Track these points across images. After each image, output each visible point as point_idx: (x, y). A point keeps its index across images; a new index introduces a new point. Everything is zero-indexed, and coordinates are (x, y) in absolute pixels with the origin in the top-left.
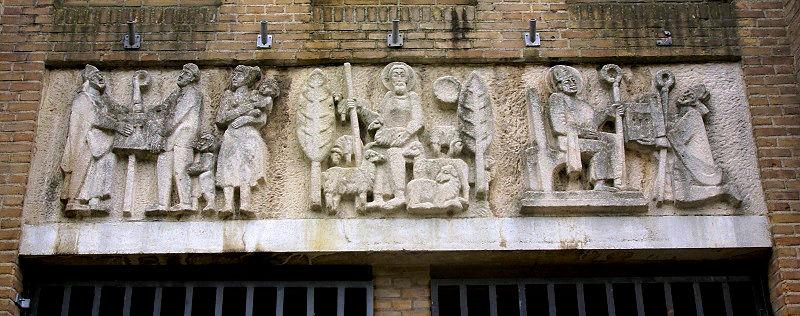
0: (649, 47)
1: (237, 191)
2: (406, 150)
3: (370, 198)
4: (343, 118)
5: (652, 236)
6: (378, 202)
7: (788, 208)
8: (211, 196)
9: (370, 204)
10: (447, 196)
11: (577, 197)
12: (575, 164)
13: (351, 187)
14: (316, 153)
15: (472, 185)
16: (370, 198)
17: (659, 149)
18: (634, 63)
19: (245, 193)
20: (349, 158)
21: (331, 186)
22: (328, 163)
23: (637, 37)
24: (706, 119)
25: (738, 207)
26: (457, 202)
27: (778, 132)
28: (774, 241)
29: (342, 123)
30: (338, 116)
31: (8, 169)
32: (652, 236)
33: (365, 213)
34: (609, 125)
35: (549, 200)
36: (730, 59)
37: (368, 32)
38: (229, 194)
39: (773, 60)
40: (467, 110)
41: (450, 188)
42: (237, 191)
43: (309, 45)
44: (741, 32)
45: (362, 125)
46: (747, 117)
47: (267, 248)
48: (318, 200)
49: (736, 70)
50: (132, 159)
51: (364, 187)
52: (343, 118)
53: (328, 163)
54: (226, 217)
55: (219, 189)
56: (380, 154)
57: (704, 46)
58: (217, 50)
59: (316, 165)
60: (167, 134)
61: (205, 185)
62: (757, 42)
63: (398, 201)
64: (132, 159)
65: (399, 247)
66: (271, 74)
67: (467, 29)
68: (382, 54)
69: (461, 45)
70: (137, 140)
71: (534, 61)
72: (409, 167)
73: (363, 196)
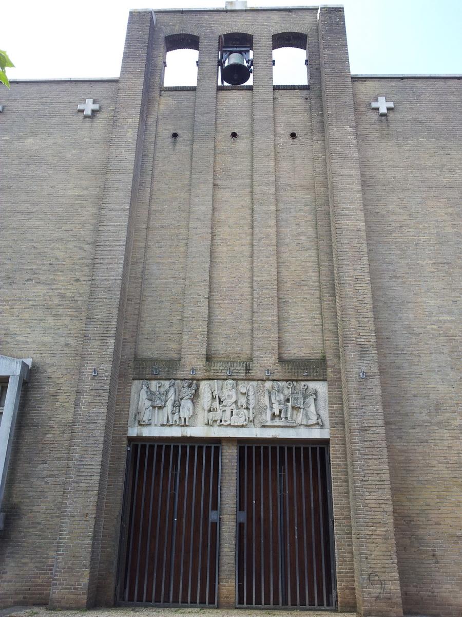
0: (301, 376)
1: (185, 419)
2: (231, 408)
3: (221, 421)
4: (214, 397)
5: (297, 435)
6: (222, 423)
7: (335, 427)
8: (178, 420)
9: (221, 423)
10: (241, 422)
11: (277, 422)
12: (277, 413)
13: (216, 418)
14: (207, 408)
15: (249, 418)
16: (221, 421)
17: (301, 408)
18: (297, 381)
19: (187, 420)
20: (215, 409)
21: (210, 418)
22: (210, 411)
23: (298, 372)
24: (315, 400)
25: (322, 426)
26: (244, 424)
27: (336, 404)
28: (331, 437)
29: (213, 398)
30: (213, 396)
31: (124, 411)
32: (297, 435)
33: (220, 426)
34: (288, 400)
35: (269, 423)
36: (324, 380)
37: (222, 370)
38: (183, 420)
39: (336, 381)
40: (248, 396)
41: (243, 419)
42: (185, 419)
43: (205, 374)
44: (328, 372)
45: (220, 399)
46: (327, 398)
47: (193, 435)
48: (207, 422)
49: (325, 384)
50: (157, 408)
51: (219, 419)
52: (214, 397)
53: (210, 411)
54: (182, 426)
55: (180, 418)
56: (224, 409)
57: (317, 376)
58: (180, 374)
59: (206, 411)
60: (166, 401)
61: (176, 417)
62: (332, 375)
63: (228, 423)
64: (157, 408)
65: (228, 436)
66: (195, 382)
67: (250, 370)
68: (226, 377)
69: (248, 375)
70: (158, 403)
71: (268, 380)
72: (232, 412)
73: (219, 421)
